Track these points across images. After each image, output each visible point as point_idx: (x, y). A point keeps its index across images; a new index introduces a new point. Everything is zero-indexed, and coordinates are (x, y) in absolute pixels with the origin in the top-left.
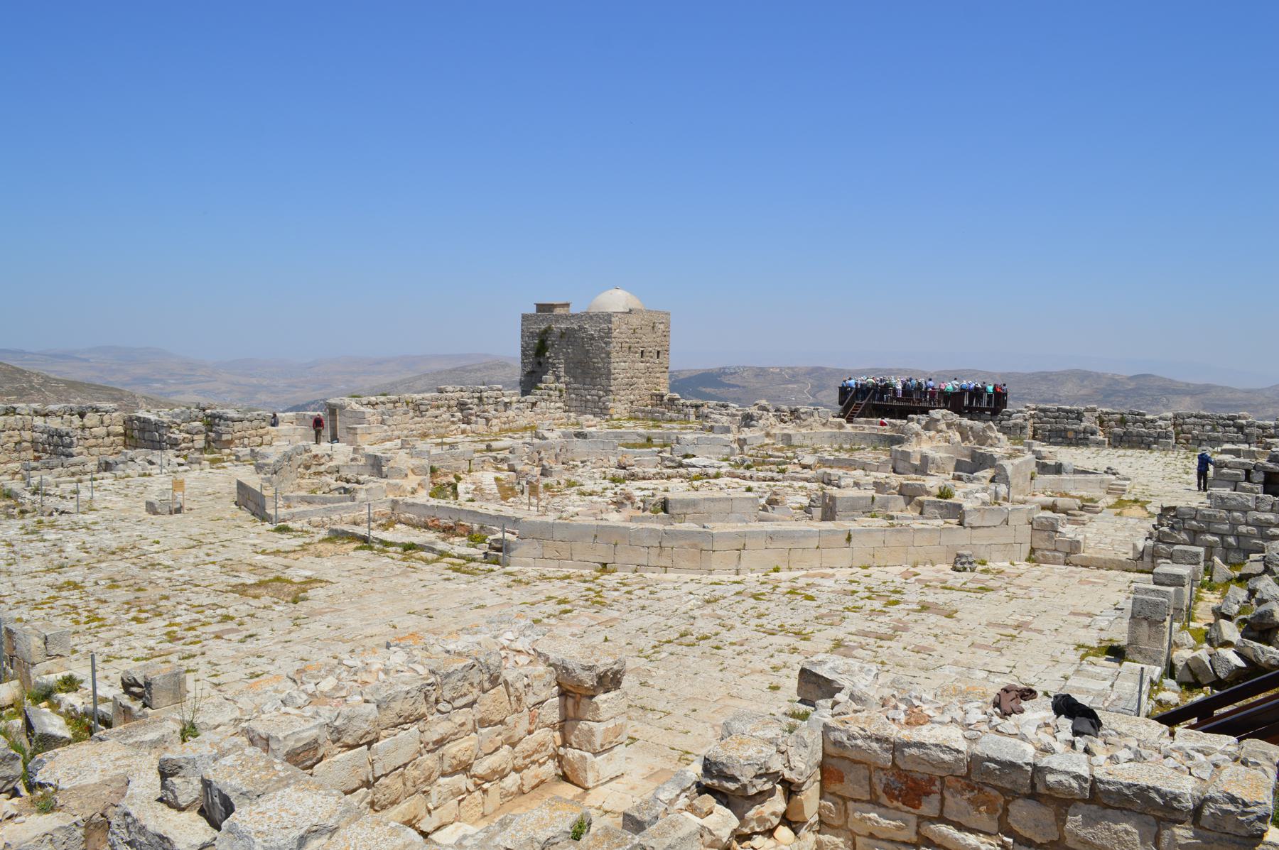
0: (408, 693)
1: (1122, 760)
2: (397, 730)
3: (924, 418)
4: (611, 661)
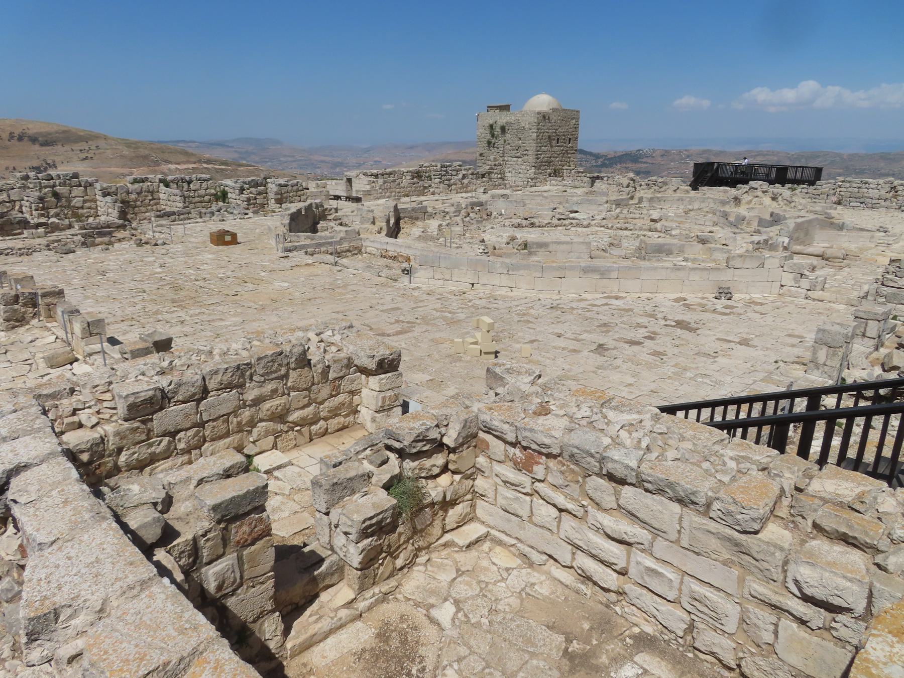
0: (227, 369)
1: (669, 459)
2: (220, 392)
3: (745, 187)
4: (388, 352)
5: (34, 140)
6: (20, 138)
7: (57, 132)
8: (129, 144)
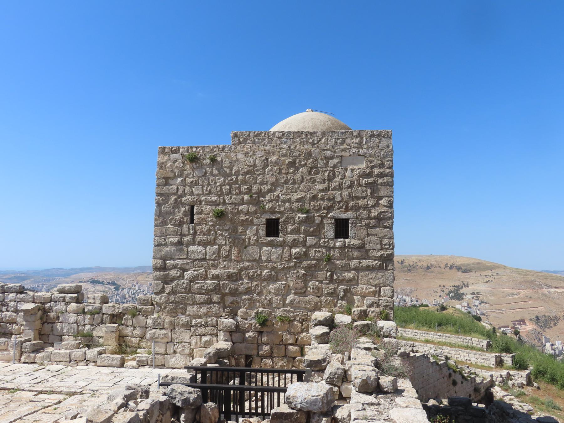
5: (459, 268)
6: (451, 268)
7: (473, 264)
8: (520, 272)
